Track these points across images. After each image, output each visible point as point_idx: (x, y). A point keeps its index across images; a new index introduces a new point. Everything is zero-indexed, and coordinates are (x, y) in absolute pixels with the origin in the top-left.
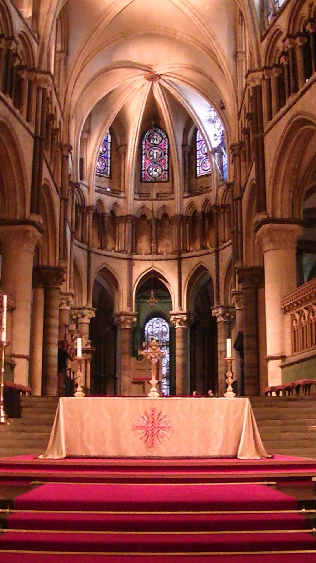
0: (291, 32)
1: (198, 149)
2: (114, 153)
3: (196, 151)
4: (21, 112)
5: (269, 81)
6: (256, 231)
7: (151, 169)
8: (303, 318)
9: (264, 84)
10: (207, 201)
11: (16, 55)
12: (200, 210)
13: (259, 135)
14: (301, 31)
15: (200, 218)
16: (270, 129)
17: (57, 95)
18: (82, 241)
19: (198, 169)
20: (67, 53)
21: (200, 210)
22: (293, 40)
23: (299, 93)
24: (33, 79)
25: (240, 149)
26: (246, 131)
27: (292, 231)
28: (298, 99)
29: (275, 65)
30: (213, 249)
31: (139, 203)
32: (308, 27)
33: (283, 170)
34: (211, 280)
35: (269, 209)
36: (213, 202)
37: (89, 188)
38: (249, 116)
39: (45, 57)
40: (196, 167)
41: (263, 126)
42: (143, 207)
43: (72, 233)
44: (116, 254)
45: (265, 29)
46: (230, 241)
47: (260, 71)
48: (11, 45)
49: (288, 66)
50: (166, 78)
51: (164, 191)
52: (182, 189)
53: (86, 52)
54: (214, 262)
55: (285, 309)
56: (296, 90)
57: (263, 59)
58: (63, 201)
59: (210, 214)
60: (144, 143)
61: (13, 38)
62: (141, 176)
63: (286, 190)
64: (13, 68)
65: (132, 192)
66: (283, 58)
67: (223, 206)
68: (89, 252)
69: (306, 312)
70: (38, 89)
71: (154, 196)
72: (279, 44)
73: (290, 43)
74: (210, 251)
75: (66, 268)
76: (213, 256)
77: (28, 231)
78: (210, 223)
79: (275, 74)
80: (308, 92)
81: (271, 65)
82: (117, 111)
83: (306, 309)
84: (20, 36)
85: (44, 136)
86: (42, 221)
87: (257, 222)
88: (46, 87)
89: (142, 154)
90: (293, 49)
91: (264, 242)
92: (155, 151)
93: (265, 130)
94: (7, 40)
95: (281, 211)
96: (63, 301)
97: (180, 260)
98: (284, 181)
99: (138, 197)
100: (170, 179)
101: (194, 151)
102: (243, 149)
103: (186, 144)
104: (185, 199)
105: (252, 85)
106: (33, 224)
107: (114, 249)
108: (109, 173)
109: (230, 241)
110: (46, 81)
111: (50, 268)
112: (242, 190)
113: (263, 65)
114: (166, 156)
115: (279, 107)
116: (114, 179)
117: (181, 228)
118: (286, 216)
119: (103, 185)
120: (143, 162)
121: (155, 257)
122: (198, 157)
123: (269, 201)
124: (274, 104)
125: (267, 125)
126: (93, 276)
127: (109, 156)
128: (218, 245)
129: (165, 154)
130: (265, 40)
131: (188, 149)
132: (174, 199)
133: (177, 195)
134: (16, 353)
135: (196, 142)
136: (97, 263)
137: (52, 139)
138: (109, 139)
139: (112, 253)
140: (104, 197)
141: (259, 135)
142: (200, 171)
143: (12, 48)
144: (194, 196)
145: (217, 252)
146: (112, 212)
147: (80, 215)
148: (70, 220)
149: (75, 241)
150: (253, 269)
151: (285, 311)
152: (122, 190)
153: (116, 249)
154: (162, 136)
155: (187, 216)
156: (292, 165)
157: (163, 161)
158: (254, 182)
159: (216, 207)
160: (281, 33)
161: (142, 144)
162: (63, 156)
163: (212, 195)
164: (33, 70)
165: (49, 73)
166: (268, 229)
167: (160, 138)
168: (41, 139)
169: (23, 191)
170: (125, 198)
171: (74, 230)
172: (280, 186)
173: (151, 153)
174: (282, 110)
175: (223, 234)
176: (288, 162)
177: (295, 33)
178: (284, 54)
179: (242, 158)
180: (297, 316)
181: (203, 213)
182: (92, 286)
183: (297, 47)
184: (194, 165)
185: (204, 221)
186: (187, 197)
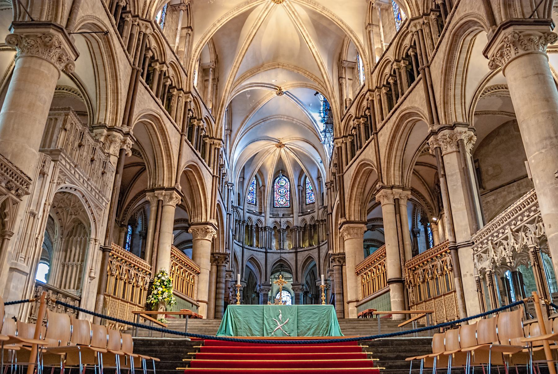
0: (357, 116)
1: (307, 188)
2: (258, 190)
3: (306, 189)
4: (205, 161)
5: (346, 143)
6: (340, 229)
7: (279, 200)
8: (368, 277)
9: (343, 146)
10: (313, 218)
11: (203, 129)
12: (308, 223)
13: (340, 175)
14: (363, 115)
15: (309, 228)
16: (347, 170)
17: (226, 154)
18: (239, 242)
19: (307, 199)
20: (231, 131)
21: (308, 223)
22: (358, 120)
23: (362, 149)
24: (212, 143)
25: (331, 185)
26: (334, 174)
27: (361, 228)
28: (362, 152)
29: (349, 135)
30: (316, 246)
31: (273, 219)
32: (367, 112)
33: (355, 194)
34: (315, 265)
35: (347, 216)
36: (316, 219)
37: (243, 210)
38: (335, 165)
39: (219, 131)
40: (306, 198)
41: (343, 169)
43: (233, 235)
44: (259, 250)
45: (343, 115)
46: (326, 241)
47: (340, 138)
48: (200, 123)
49: (356, 135)
50: (288, 146)
51: (287, 213)
52: (298, 211)
53: (242, 130)
54: (317, 254)
55: (358, 273)
56: (361, 148)
57: (342, 132)
58: (228, 215)
59: (314, 226)
60: (275, 184)
61: (201, 119)
62: (274, 204)
63: (357, 205)
64: (201, 136)
65: (269, 213)
66: (353, 130)
67: (322, 221)
68: (243, 247)
69: (369, 273)
70: (215, 148)
71: (281, 216)
72: (351, 123)
73: (357, 122)
74: (314, 247)
75: (230, 254)
76: (317, 250)
77: (208, 228)
78: (314, 231)
79: (349, 140)
80: (367, 148)
81: (347, 135)
82: (260, 165)
83: (370, 271)
84: (205, 118)
85: (218, 175)
86: (216, 224)
87: (340, 223)
88: (220, 147)
89: (274, 191)
90: (359, 125)
91: (344, 235)
92: (282, 189)
93: (344, 171)
94: (197, 120)
95: (354, 216)
96: (227, 275)
97: (296, 253)
98: (355, 200)
99: (271, 216)
100: (291, 206)
101: (305, 189)
102: (332, 185)
103: (300, 185)
104: (299, 217)
105: (336, 146)
106: (211, 224)
107: (258, 246)
108: (255, 202)
109: (326, 241)
110: (219, 144)
111: (220, 254)
112: (332, 210)
113: (342, 135)
114: (289, 192)
115: (352, 157)
116: (258, 206)
117: (298, 234)
118: (357, 220)
119: (253, 209)
120: (275, 196)
121: (282, 251)
122: (307, 192)
123: (347, 211)
124: (349, 157)
125: (345, 169)
126: (245, 263)
127: (255, 192)
128: (319, 243)
129: (288, 191)
130: (344, 121)
131: (301, 188)
132: (293, 217)
133: (295, 215)
134: (200, 299)
135: (306, 184)
136: (247, 254)
137: (223, 179)
138: (255, 183)
139: (257, 249)
140: (252, 216)
141: (340, 175)
142: (308, 201)
143: (201, 125)
144: (305, 215)
145: (319, 247)
146: (257, 225)
147: (238, 226)
148: (232, 228)
149: (235, 240)
150: (339, 254)
151: (358, 274)
152: (263, 212)
153: (259, 246)
154: (285, 180)
155: (301, 227)
156: (359, 190)
157: (287, 195)
158: (339, 202)
159: (317, 220)
160: (352, 116)
161: (274, 185)
162: (228, 189)
164: (213, 138)
165: (221, 140)
166: (347, 228)
167: (284, 182)
168: (216, 177)
170: (264, 217)
171: (234, 233)
172: (353, 202)
173: (280, 190)
174: (353, 159)
175: (322, 237)
176: (357, 188)
177: (360, 116)
178: (354, 128)
179: (332, 190)
180: (365, 276)
181: (310, 225)
182: (244, 268)
183: (361, 124)
184: (305, 197)
185: (311, 230)
186: (302, 216)
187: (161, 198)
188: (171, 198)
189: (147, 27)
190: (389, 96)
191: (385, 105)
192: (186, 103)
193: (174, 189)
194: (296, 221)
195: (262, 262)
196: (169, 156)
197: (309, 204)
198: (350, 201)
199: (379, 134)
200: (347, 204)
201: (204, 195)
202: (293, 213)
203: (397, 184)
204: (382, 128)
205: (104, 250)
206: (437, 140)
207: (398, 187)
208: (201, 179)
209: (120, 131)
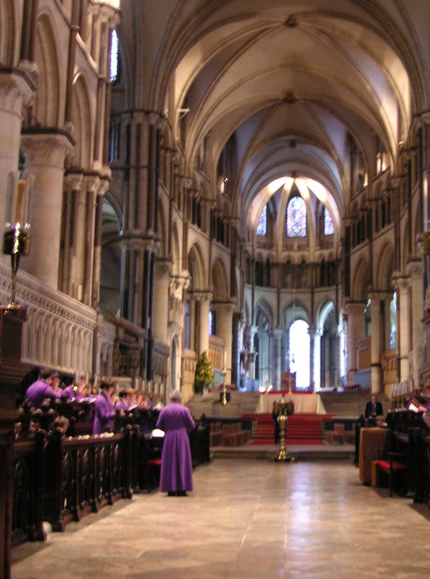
12: (326, 259)
21: (326, 259)
31: (286, 253)
36: (334, 257)
42: (289, 256)
71: (296, 247)
97: (313, 293)
99: (285, 249)
108: (265, 231)
125: (352, 251)
132: (309, 251)
146: (268, 260)
159: (337, 260)
163: (334, 250)
169: (227, 285)
174: (358, 247)
181: (329, 263)
187: (199, 299)
188: (206, 299)
189: (188, 183)
190: (383, 206)
191: (380, 216)
192: (211, 211)
193: (208, 291)
194: (313, 254)
195: (274, 304)
196: (203, 263)
197: (328, 235)
198: (354, 281)
199: (374, 242)
200: (351, 284)
201: (225, 275)
202: (308, 245)
203: (384, 288)
204: (376, 239)
205: (182, 359)
206: (397, 284)
207: (384, 291)
208: (223, 265)
209: (182, 277)
